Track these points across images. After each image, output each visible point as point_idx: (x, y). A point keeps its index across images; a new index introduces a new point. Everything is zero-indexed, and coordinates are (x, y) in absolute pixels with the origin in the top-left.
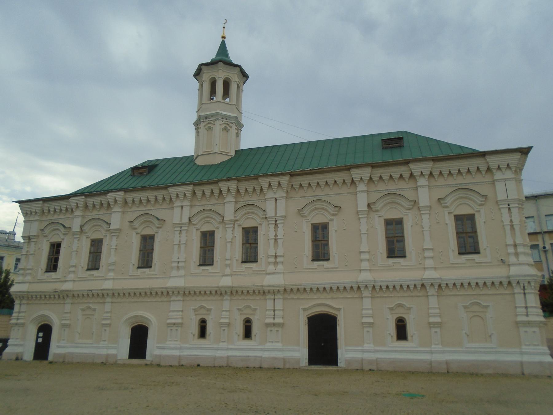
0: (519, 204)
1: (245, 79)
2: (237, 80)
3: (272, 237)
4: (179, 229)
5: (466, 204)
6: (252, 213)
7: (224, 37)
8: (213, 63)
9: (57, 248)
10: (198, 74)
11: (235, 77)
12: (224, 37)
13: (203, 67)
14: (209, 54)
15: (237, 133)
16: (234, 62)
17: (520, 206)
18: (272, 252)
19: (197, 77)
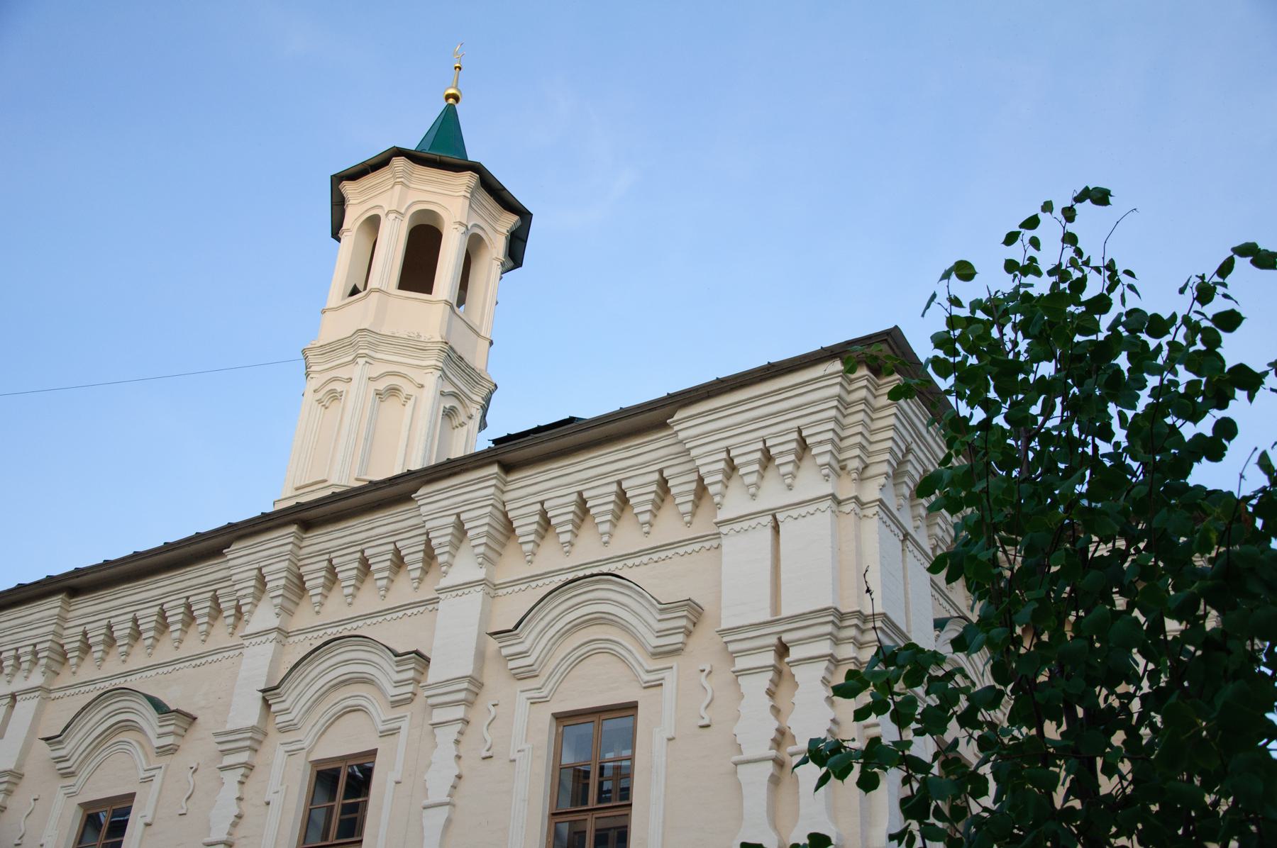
6: (345, 683)
9: (109, 835)
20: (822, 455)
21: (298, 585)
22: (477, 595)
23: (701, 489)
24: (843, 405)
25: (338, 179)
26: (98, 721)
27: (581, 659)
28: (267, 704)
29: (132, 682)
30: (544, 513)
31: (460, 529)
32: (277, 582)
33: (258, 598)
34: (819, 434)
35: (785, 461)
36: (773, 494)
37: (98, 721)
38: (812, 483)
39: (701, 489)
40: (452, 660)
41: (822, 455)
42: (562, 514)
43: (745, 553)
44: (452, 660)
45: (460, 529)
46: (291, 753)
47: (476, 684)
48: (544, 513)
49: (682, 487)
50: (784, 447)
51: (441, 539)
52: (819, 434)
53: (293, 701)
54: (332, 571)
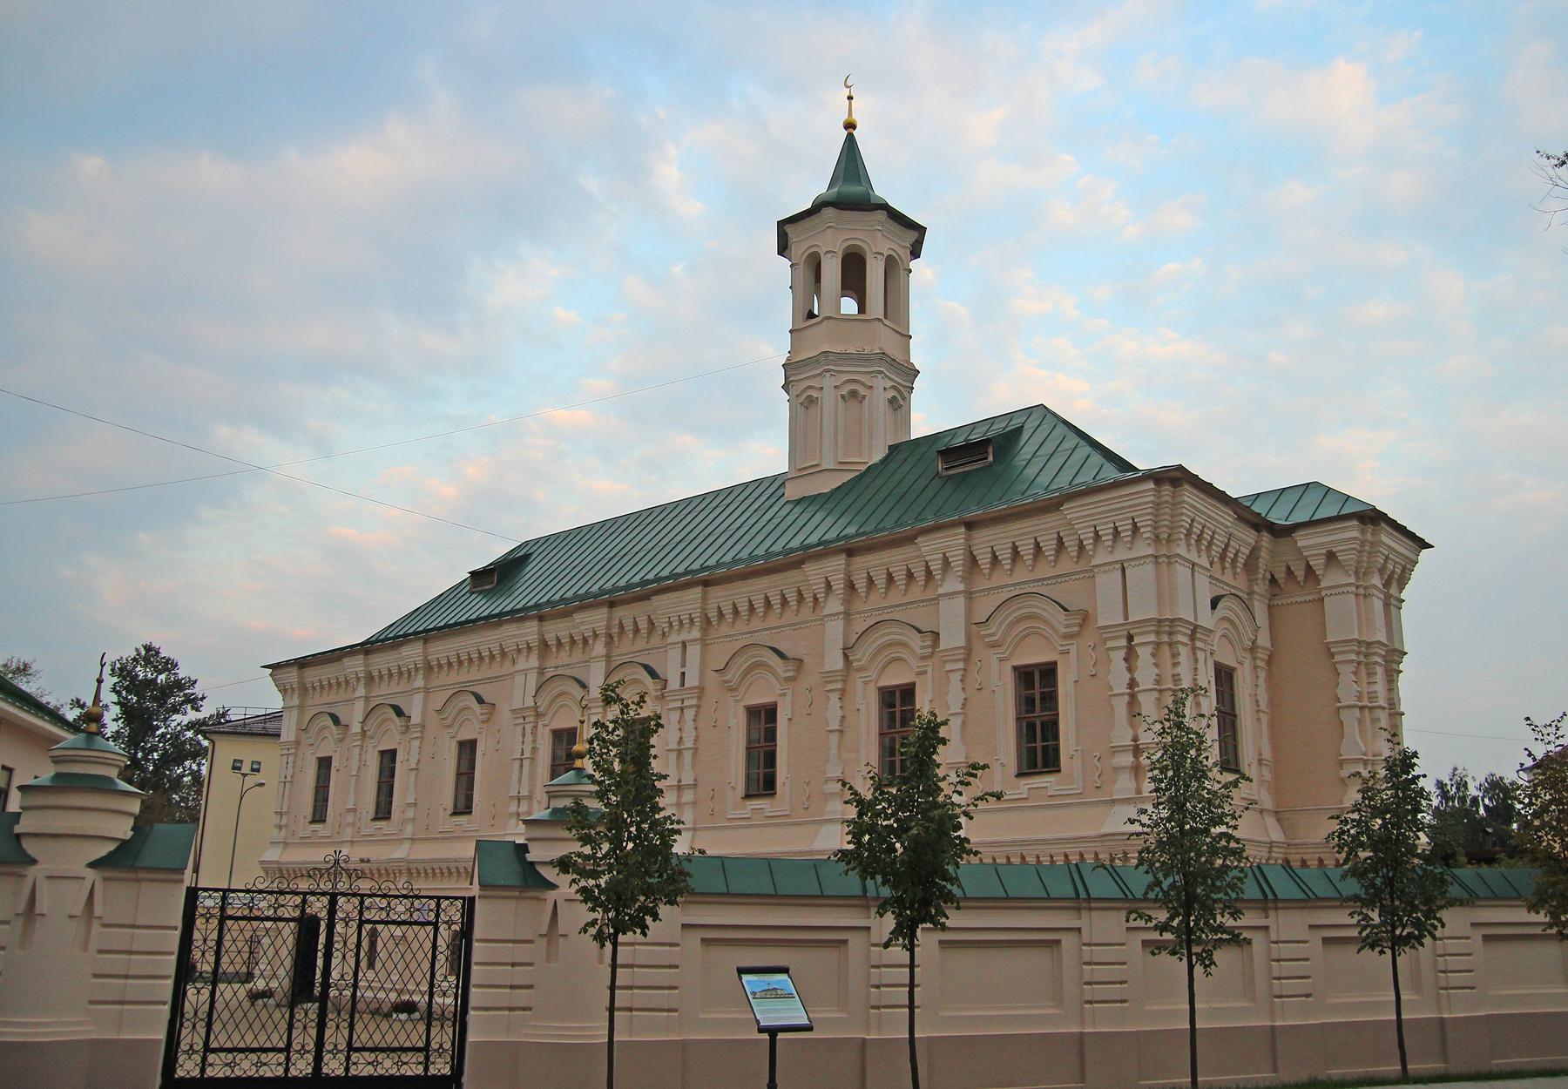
7: (850, 126)
12: (850, 126)
13: (789, 229)
14: (809, 184)
20: (1146, 532)
21: (851, 586)
22: (961, 600)
23: (1081, 547)
24: (1158, 505)
25: (781, 224)
26: (743, 662)
27: (1024, 637)
28: (846, 657)
29: (756, 638)
30: (994, 553)
31: (946, 562)
32: (839, 585)
33: (827, 595)
34: (1144, 522)
35: (1126, 535)
36: (1121, 554)
37: (743, 662)
38: (1143, 549)
39: (1081, 547)
40: (953, 638)
41: (1146, 532)
42: (1005, 554)
43: (1108, 583)
44: (953, 638)
45: (946, 562)
46: (866, 683)
47: (968, 654)
48: (994, 553)
49: (1072, 548)
50: (1125, 528)
51: (936, 566)
52: (1144, 522)
53: (861, 656)
54: (870, 581)
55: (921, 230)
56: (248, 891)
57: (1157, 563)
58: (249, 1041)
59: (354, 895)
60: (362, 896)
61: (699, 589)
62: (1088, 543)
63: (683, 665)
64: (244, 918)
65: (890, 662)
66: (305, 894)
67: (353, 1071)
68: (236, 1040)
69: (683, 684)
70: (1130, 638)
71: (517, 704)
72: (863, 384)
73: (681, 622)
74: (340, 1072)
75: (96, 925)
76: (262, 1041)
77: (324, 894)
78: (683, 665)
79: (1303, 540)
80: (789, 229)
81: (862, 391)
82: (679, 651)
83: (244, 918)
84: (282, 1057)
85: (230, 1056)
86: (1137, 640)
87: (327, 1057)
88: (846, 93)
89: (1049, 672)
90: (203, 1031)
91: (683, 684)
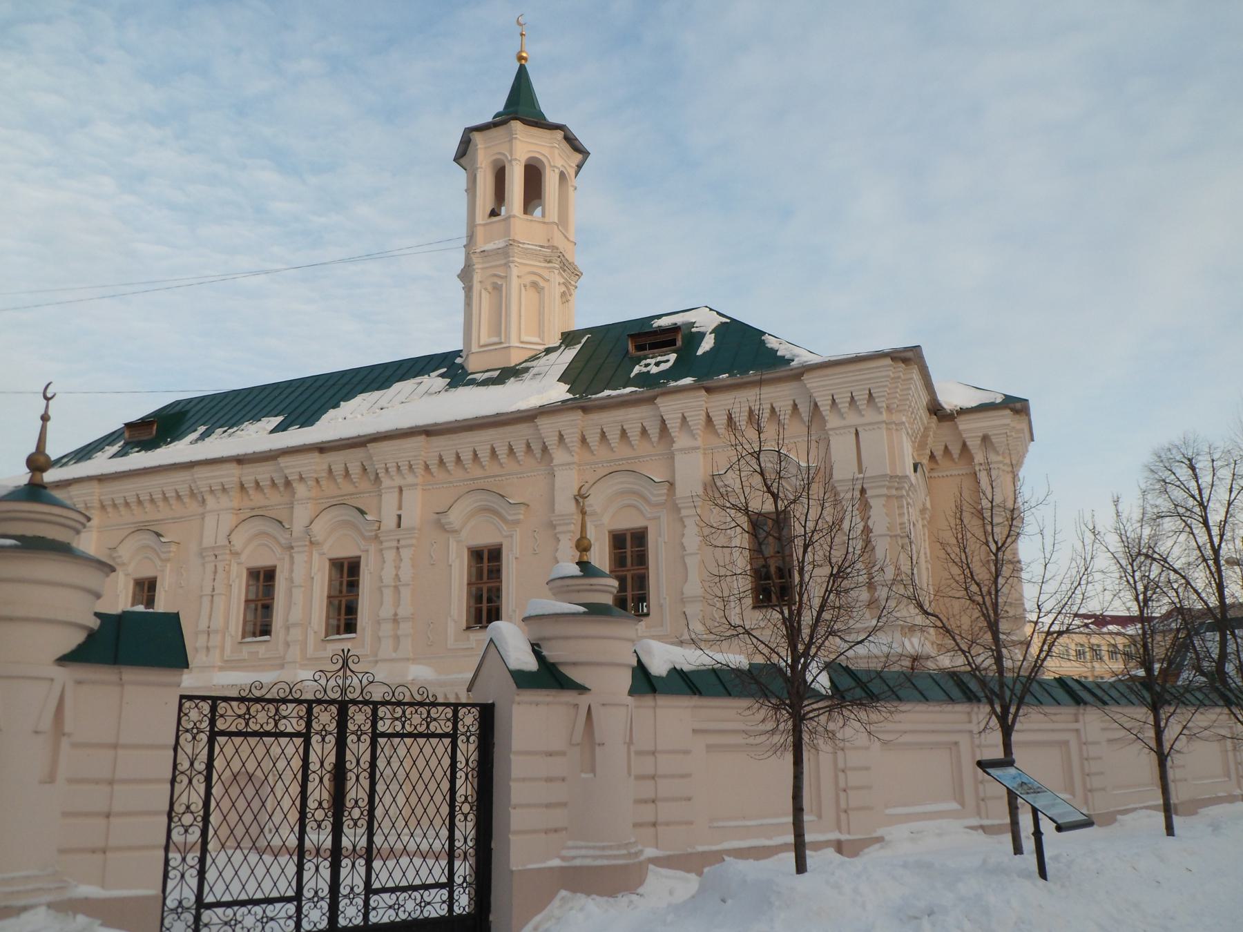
0: (889, 488)
1: (579, 157)
2: (559, 163)
3: (208, 590)
4: (395, 544)
5: (634, 506)
8: (500, 121)
10: (464, 152)
11: (555, 156)
12: (520, 58)
13: (477, 137)
15: (563, 294)
16: (552, 118)
17: (894, 492)
18: (387, 611)
19: (462, 161)
55: (585, 153)
56: (241, 700)
57: (888, 429)
58: (252, 891)
59: (366, 703)
60: (375, 705)
61: (422, 438)
62: (825, 406)
63: (400, 508)
64: (239, 734)
65: (629, 506)
66: (310, 703)
67: (374, 918)
68: (236, 892)
69: (399, 526)
70: (863, 491)
71: (208, 541)
72: (540, 276)
73: (398, 467)
74: (359, 921)
75: (65, 742)
76: (268, 890)
77: (332, 702)
78: (400, 508)
79: (964, 424)
80: (477, 137)
81: (542, 283)
82: (396, 495)
83: (239, 734)
84: (291, 908)
85: (230, 912)
86: (869, 493)
87: (343, 903)
88: (519, 29)
89: (640, 537)
90: (194, 883)
91: (399, 526)
